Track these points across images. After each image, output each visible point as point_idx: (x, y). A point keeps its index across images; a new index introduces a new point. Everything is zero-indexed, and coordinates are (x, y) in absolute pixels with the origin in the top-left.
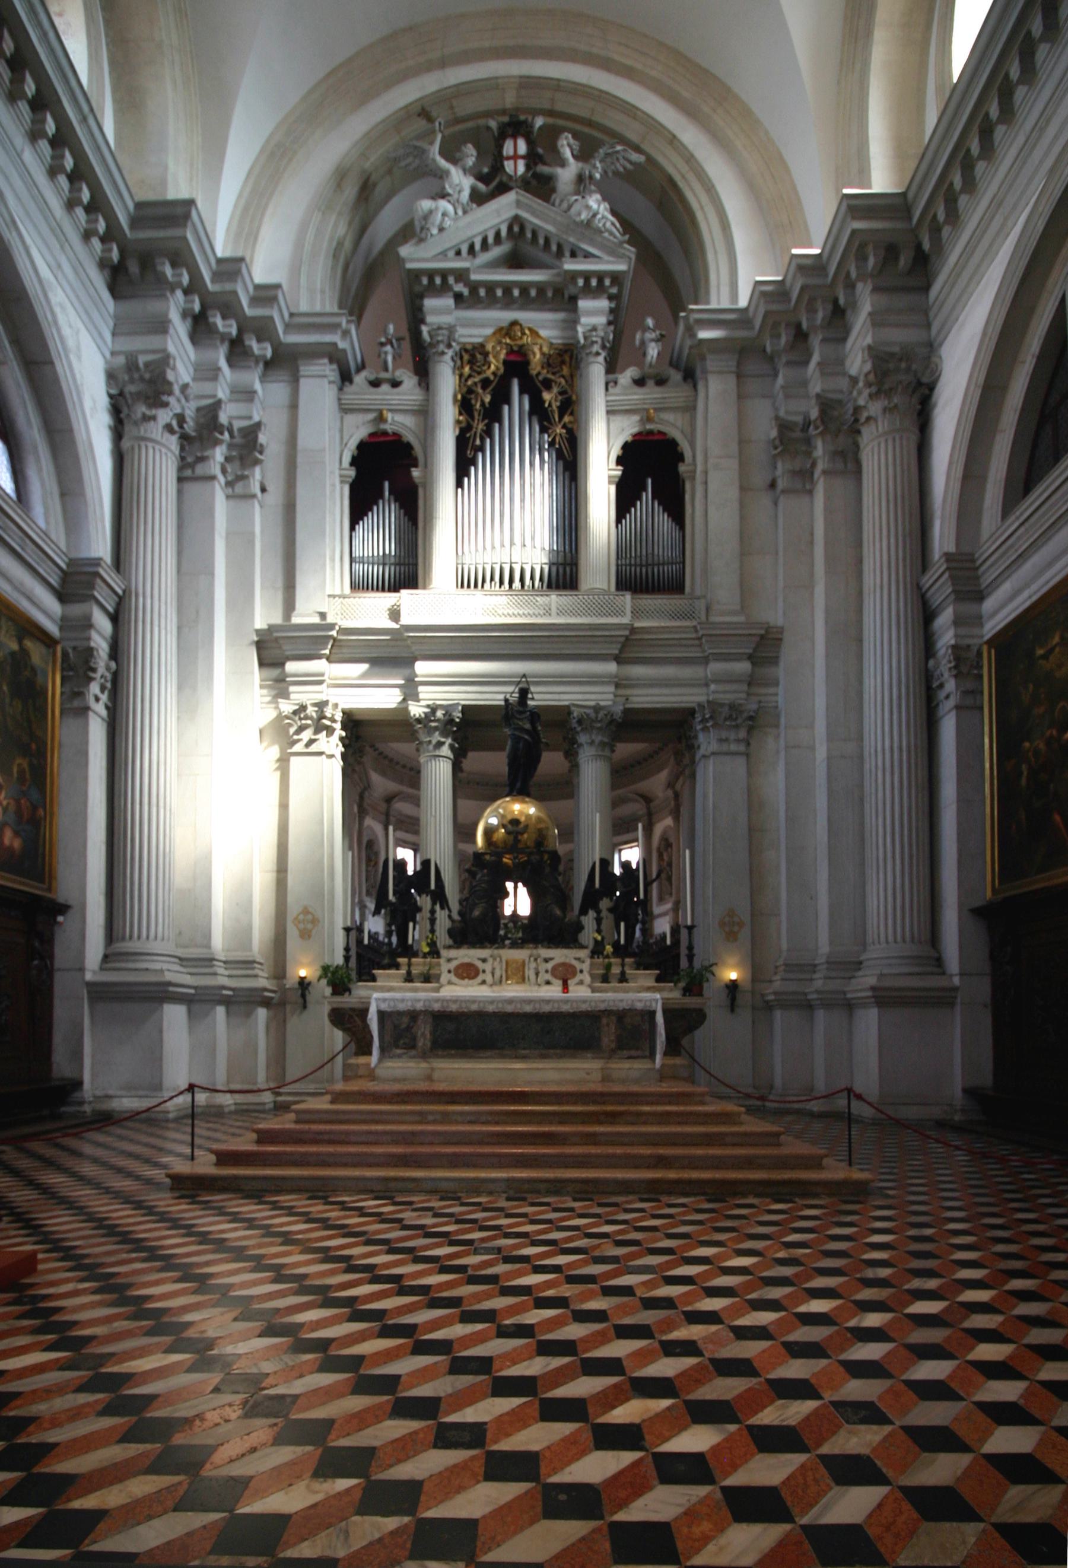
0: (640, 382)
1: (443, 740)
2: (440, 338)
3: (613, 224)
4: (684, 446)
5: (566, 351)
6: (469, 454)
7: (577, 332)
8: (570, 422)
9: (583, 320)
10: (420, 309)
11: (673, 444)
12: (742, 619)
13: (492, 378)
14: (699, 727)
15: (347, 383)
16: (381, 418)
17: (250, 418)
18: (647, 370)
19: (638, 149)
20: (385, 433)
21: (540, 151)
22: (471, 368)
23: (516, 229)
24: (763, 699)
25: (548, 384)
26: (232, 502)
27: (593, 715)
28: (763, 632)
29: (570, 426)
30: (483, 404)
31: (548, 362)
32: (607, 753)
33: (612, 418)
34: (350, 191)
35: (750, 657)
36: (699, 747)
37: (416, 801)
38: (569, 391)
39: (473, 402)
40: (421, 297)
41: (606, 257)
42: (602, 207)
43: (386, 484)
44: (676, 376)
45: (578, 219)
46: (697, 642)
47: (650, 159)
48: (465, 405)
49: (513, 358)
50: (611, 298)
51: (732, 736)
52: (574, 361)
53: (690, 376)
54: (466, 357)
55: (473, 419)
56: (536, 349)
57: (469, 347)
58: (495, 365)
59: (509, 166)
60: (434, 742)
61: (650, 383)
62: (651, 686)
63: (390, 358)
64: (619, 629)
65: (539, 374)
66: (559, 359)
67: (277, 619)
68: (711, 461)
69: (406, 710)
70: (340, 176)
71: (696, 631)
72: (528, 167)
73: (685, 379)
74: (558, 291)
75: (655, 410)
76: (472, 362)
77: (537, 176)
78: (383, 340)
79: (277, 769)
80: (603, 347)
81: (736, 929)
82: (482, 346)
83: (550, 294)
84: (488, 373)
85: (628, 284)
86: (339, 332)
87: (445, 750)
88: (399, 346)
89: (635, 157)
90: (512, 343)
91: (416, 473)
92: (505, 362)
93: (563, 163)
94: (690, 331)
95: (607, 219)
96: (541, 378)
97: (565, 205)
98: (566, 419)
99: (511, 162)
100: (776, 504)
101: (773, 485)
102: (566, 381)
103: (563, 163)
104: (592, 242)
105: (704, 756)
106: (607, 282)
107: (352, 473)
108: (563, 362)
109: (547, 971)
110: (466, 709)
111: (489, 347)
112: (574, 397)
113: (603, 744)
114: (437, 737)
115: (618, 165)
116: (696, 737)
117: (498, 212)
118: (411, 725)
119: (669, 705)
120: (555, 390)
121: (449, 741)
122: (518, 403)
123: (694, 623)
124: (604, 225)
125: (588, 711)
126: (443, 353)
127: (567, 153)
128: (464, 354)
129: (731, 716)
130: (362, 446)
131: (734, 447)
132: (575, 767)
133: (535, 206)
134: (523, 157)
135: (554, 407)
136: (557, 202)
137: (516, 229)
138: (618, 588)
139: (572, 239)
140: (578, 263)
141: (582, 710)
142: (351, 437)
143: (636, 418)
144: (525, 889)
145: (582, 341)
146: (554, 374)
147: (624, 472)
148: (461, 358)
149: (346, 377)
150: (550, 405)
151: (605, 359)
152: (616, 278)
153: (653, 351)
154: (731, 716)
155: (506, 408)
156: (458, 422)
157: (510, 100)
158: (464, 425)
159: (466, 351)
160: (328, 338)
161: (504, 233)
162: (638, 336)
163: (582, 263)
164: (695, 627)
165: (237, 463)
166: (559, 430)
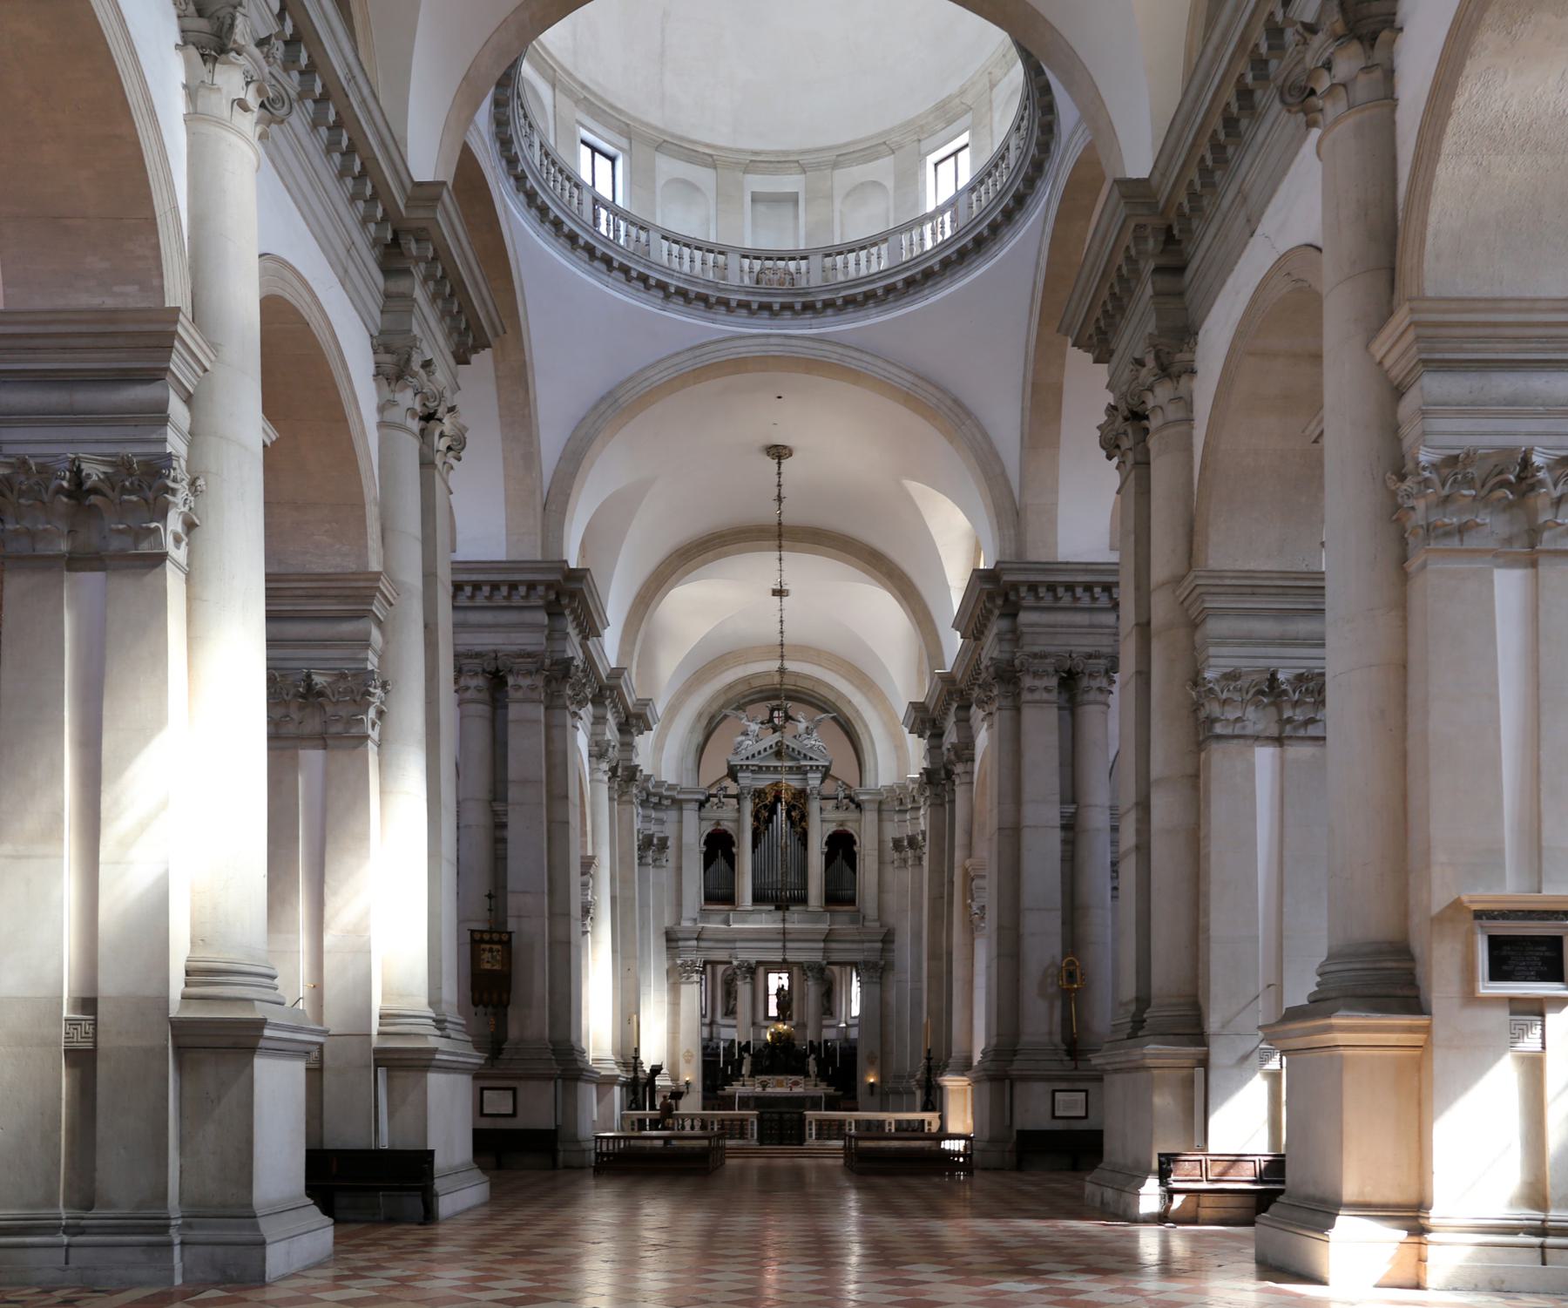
11: (851, 836)
34: (704, 722)
44: (853, 806)
58: (770, 798)
59: (776, 721)
70: (700, 715)
74: (799, 768)
76: (759, 797)
82: (763, 789)
84: (767, 802)
98: (803, 824)
152: (823, 766)
166: (799, 830)
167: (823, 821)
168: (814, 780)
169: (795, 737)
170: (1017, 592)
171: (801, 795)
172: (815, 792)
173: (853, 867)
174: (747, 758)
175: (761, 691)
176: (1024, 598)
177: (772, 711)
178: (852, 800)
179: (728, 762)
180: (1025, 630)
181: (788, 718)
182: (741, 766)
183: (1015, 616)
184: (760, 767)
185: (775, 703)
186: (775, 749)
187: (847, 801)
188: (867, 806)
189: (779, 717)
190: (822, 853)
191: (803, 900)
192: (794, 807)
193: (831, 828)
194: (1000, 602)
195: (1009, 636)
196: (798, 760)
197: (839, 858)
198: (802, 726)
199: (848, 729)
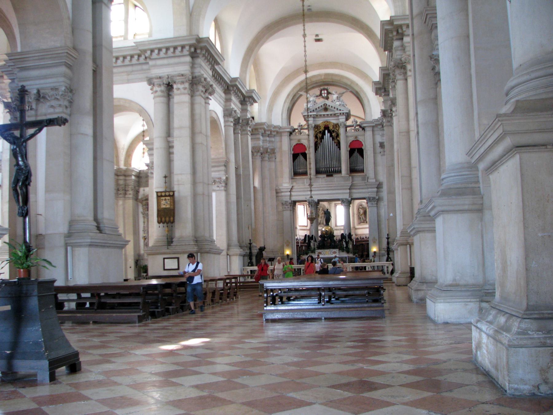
23: (325, 105)
25: (333, 131)
35: (377, 188)
44: (361, 129)
48: (316, 137)
54: (316, 127)
58: (322, 129)
59: (323, 95)
74: (335, 114)
76: (317, 128)
82: (319, 125)
83: (333, 115)
84: (321, 130)
98: (338, 138)
101: (381, 152)
106: (345, 114)
108: (337, 127)
122: (327, 135)
135: (335, 137)
137: (325, 105)
152: (346, 113)
155: (325, 136)
156: (315, 140)
166: (336, 141)
167: (347, 137)
168: (342, 119)
169: (332, 101)
170: (402, 29)
171: (337, 126)
172: (342, 124)
173: (362, 156)
174: (311, 112)
175: (316, 83)
176: (405, 31)
177: (321, 91)
178: (360, 127)
179: (302, 114)
180: (406, 45)
181: (328, 93)
183: (402, 39)
184: (317, 115)
185: (322, 88)
186: (323, 107)
187: (358, 127)
188: (367, 129)
189: (324, 93)
190: (347, 151)
191: (340, 172)
192: (333, 131)
193: (352, 139)
194: (395, 33)
195: (400, 48)
196: (334, 111)
198: (335, 97)
199: (358, 96)
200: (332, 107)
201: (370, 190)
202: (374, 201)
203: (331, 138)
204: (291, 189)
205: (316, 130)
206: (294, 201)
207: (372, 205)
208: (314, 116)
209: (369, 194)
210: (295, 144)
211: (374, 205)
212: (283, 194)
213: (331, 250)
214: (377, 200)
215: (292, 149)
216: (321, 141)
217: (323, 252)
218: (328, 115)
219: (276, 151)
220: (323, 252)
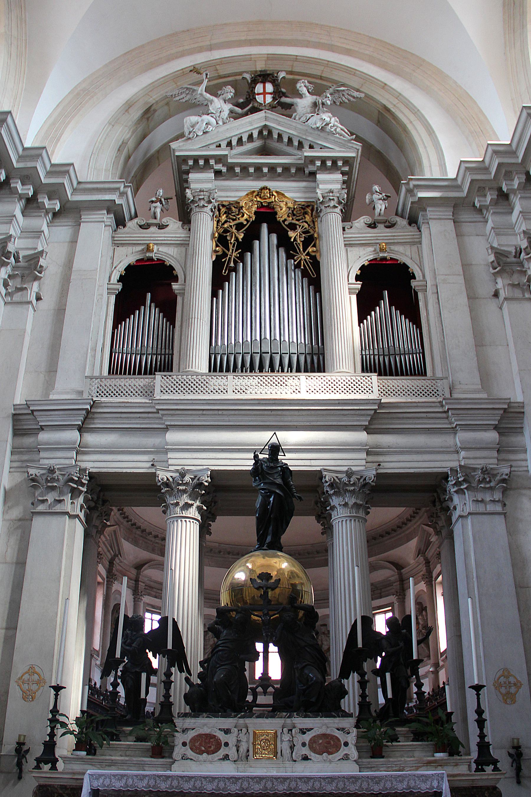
0: (372, 226)
1: (190, 502)
2: (201, 197)
3: (341, 129)
4: (414, 268)
5: (308, 206)
6: (224, 273)
7: (317, 193)
8: (313, 252)
9: (321, 186)
10: (186, 181)
11: (405, 267)
12: (484, 396)
13: (245, 223)
14: (453, 490)
15: (120, 227)
16: (148, 249)
17: (36, 248)
18: (376, 217)
19: (358, 90)
20: (151, 259)
21: (283, 90)
22: (227, 217)
23: (265, 133)
24: (513, 464)
25: (293, 227)
26: (9, 307)
27: (345, 479)
28: (506, 406)
29: (313, 254)
30: (237, 239)
31: (293, 213)
32: (361, 514)
33: (349, 249)
36: (455, 508)
37: (161, 566)
38: (311, 231)
39: (228, 238)
40: (187, 173)
41: (337, 149)
42: (333, 119)
43: (149, 295)
44: (402, 222)
45: (314, 126)
46: (444, 415)
47: (367, 96)
49: (262, 210)
50: (343, 173)
51: (488, 498)
52: (314, 213)
53: (413, 221)
54: (223, 210)
55: (229, 251)
56: (282, 205)
57: (224, 203)
59: (260, 99)
60: (181, 504)
61: (381, 226)
62: (402, 453)
63: (158, 211)
64: (367, 404)
65: (285, 220)
66: (302, 211)
67: (37, 396)
68: (439, 278)
69: (154, 475)
71: (442, 406)
72: (274, 99)
73: (410, 224)
74: (300, 169)
75: (386, 243)
76: (228, 212)
77: (281, 104)
78: (154, 199)
79: (17, 528)
80: (340, 203)
81: (513, 690)
83: (293, 171)
84: (242, 220)
85: (356, 165)
86: (118, 193)
87: (193, 512)
88: (167, 203)
89: (356, 94)
90: (262, 201)
91: (175, 286)
92: (256, 213)
93: (300, 96)
94: (410, 192)
95: (337, 127)
96: (286, 223)
97: (303, 119)
98: (310, 249)
99: (262, 96)
100: (501, 308)
101: (496, 295)
102: (309, 225)
103: (301, 96)
104: (326, 139)
105: (460, 516)
106: (340, 163)
107: (120, 287)
108: (306, 213)
109: (304, 745)
110: (214, 474)
111: (242, 204)
112: (316, 235)
113: (356, 506)
114: (185, 499)
115: (344, 99)
116: (451, 499)
117: (251, 123)
118: (159, 489)
119: (422, 470)
120: (299, 230)
121: (198, 503)
123: (440, 399)
124: (335, 130)
125: (340, 476)
126: (204, 206)
127: (304, 90)
128: (221, 208)
129: (484, 479)
130: (129, 268)
131: (459, 268)
132: (328, 529)
133: (279, 119)
134: (270, 94)
136: (297, 118)
137: (265, 133)
138: (363, 371)
139: (310, 139)
140: (315, 152)
141: (335, 475)
142: (120, 262)
143: (371, 249)
144: (276, 649)
145: (321, 199)
146: (298, 220)
147: (362, 285)
148: (219, 210)
149: (120, 222)
150: (295, 240)
151: (341, 210)
152: (347, 161)
153: (381, 206)
154: (484, 479)
155: (257, 243)
156: (215, 251)
157: (260, 66)
158: (220, 253)
159: (223, 206)
160: (107, 197)
161: (255, 135)
162: (368, 197)
163: (319, 152)
164: (440, 402)
165: (19, 280)
182: (196, 159)
184: (231, 168)
189: (264, 93)
197: (385, 303)
200: (290, 140)
201: (462, 436)
202: (491, 488)
203: (282, 251)
204: (89, 415)
205: (224, 218)
206: (92, 476)
207: (481, 508)
208: (219, 167)
209: (463, 454)
210: (131, 259)
211: (490, 508)
212: (43, 436)
213: (301, 722)
214: (504, 481)
215: (116, 276)
216: (241, 258)
217: (231, 739)
218: (272, 168)
219: (42, 262)
220: (231, 739)
